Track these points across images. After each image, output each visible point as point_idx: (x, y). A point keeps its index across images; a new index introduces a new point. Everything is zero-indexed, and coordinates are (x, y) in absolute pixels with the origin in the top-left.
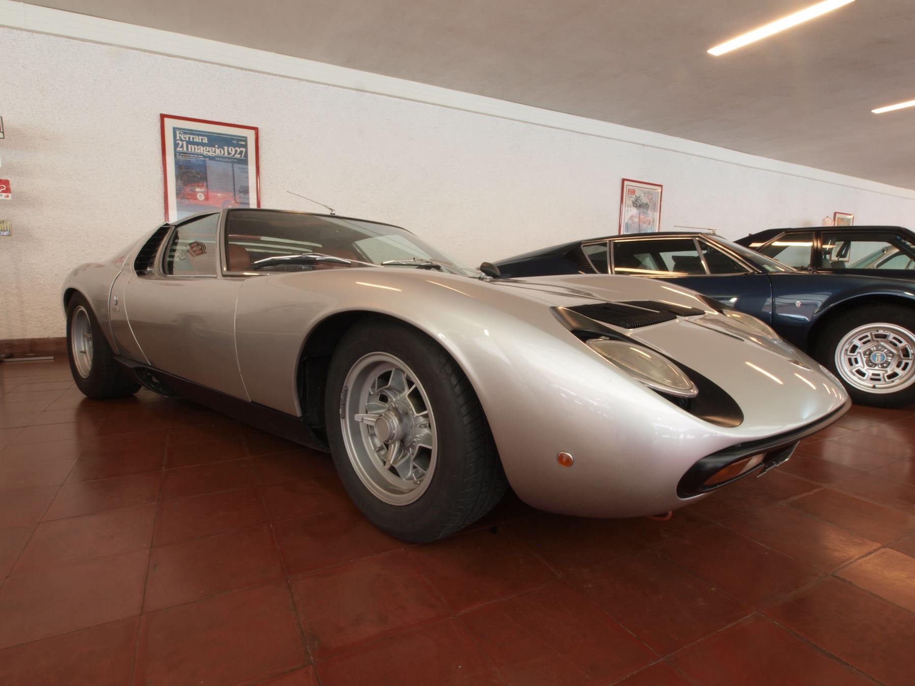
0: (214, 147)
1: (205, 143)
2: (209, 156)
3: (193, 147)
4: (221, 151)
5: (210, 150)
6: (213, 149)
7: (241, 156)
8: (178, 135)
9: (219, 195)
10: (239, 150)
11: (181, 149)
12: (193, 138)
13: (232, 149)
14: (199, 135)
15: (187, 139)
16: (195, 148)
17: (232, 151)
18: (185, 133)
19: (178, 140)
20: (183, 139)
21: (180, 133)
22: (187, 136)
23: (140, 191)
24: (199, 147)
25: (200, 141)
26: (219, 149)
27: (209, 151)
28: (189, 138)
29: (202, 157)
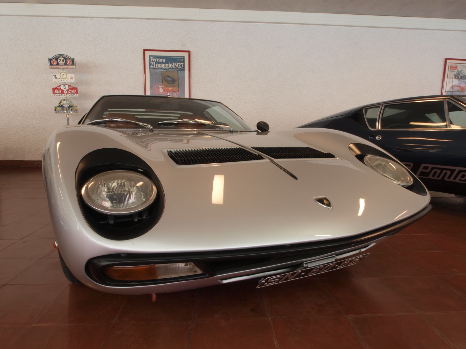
0: (168, 64)
1: (164, 62)
2: (166, 68)
3: (158, 64)
4: (171, 65)
5: (166, 65)
6: (168, 65)
7: (181, 67)
8: (151, 59)
9: (170, 88)
10: (180, 64)
11: (153, 66)
12: (158, 60)
13: (177, 64)
14: (161, 58)
15: (155, 61)
16: (159, 65)
17: (177, 65)
18: (155, 58)
19: (151, 62)
20: (153, 61)
21: (152, 58)
22: (155, 59)
23: (134, 89)
24: (161, 65)
25: (162, 61)
26: (171, 65)
27: (166, 66)
28: (156, 60)
29: (162, 69)
